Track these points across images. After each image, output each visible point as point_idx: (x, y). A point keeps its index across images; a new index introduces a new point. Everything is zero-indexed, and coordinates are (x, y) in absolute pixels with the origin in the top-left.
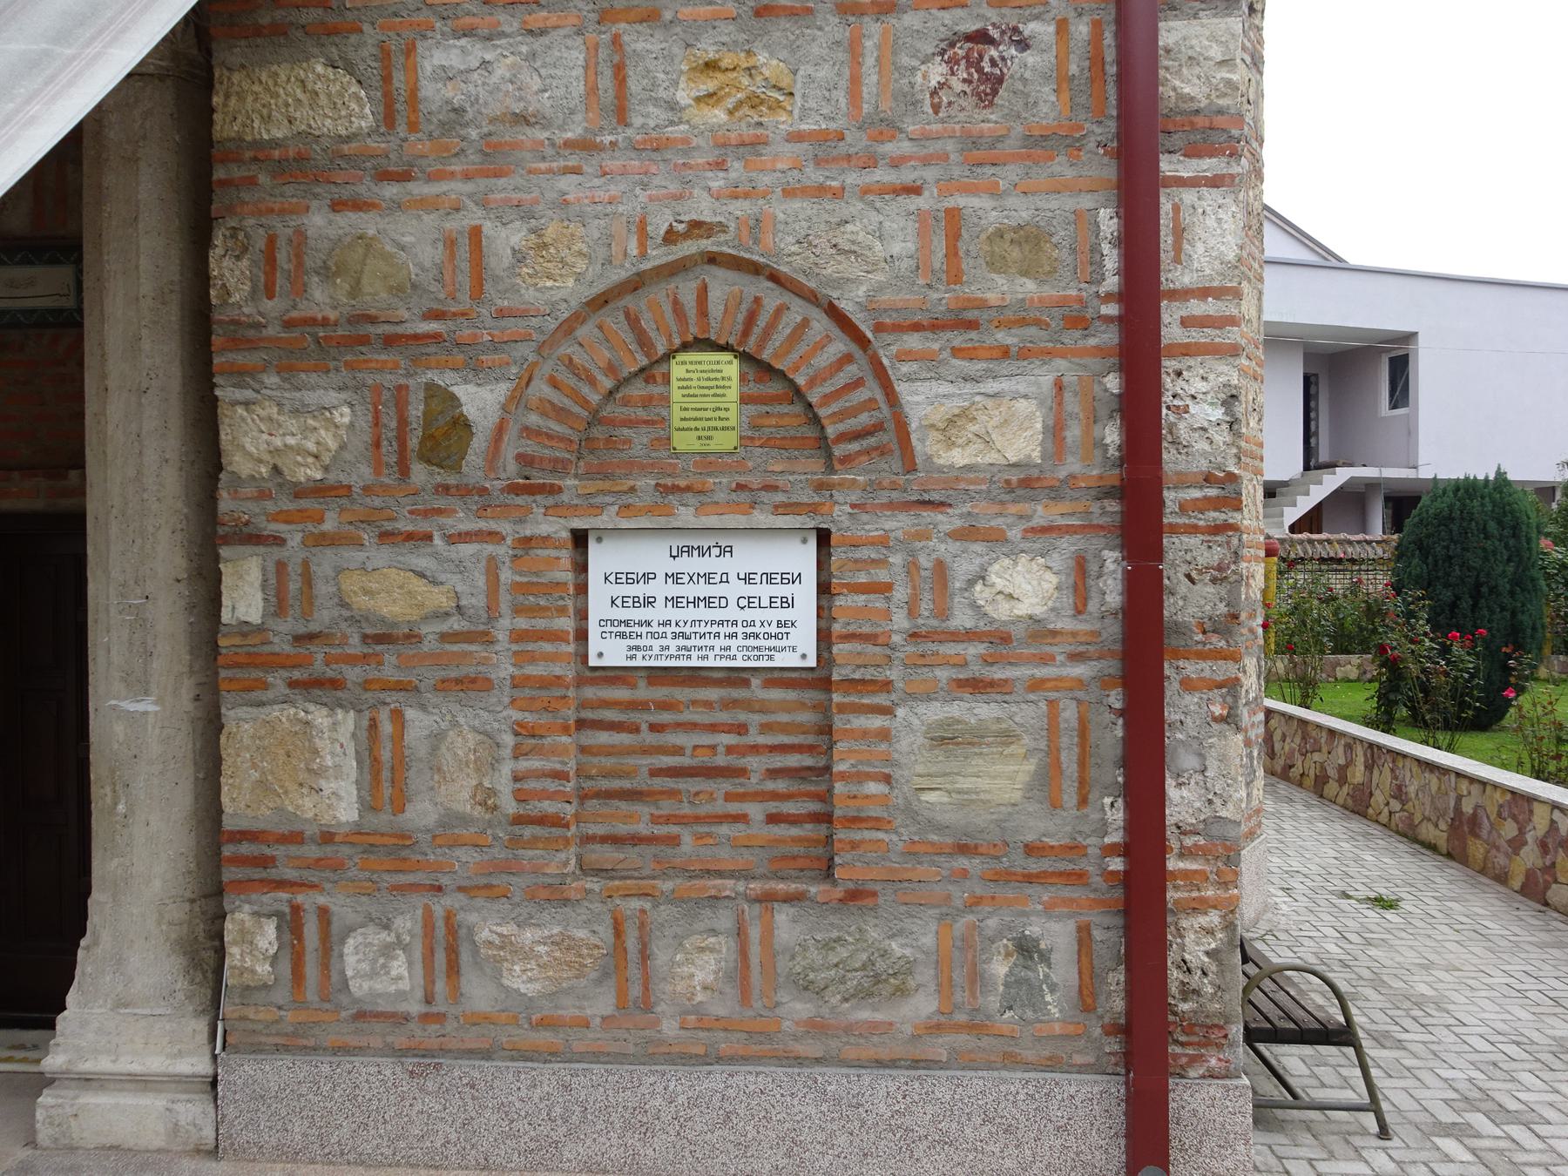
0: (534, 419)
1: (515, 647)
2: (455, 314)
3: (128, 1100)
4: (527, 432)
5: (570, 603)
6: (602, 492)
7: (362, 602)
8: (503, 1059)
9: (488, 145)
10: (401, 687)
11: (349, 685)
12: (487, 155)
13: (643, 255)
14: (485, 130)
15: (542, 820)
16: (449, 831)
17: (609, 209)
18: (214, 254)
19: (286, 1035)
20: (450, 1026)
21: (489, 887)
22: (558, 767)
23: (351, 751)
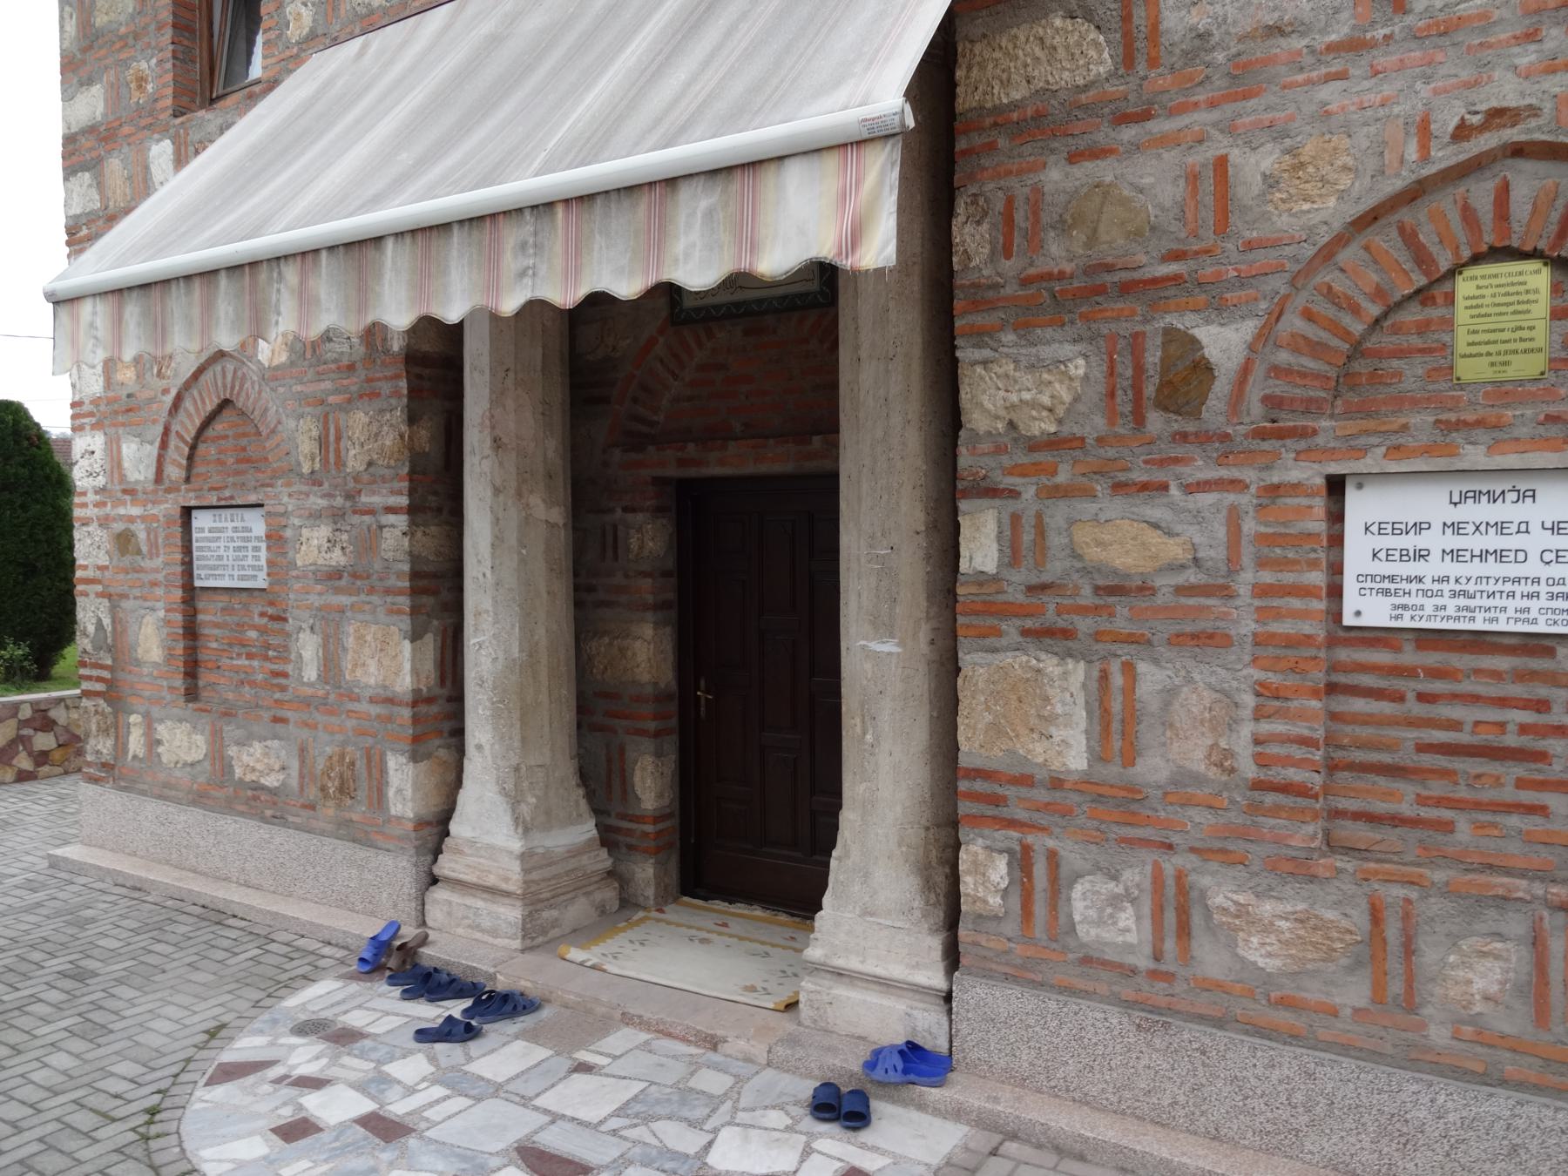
0: (1283, 357)
1: (1257, 603)
2: (1197, 253)
3: (873, 998)
4: (1277, 371)
5: (1322, 555)
6: (1367, 432)
7: (1093, 553)
8: (1238, 1031)
9: (1237, 66)
10: (1131, 639)
11: (1080, 635)
12: (1235, 77)
13: (1425, 157)
14: (1234, 51)
15: (1285, 788)
16: (1181, 790)
17: (1381, 113)
18: (957, 223)
19: (1015, 966)
20: (1180, 987)
21: (1223, 851)
22: (1306, 732)
23: (1081, 700)
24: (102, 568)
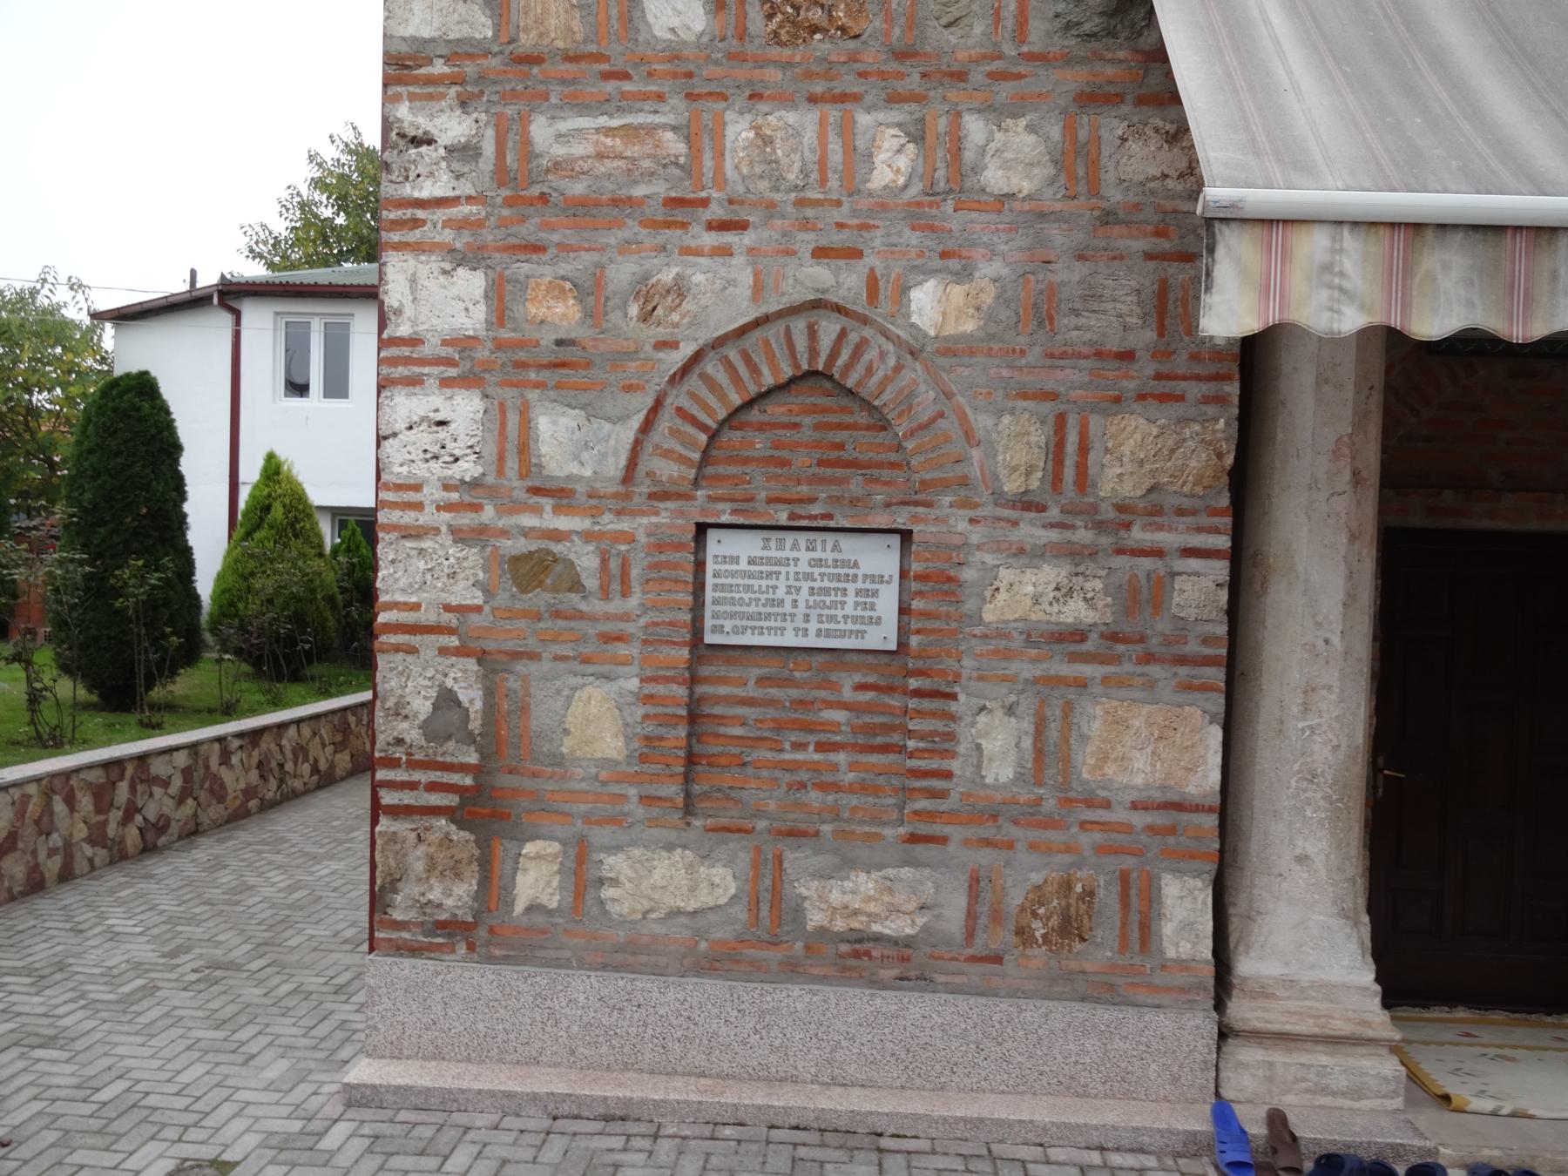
24: (460, 609)
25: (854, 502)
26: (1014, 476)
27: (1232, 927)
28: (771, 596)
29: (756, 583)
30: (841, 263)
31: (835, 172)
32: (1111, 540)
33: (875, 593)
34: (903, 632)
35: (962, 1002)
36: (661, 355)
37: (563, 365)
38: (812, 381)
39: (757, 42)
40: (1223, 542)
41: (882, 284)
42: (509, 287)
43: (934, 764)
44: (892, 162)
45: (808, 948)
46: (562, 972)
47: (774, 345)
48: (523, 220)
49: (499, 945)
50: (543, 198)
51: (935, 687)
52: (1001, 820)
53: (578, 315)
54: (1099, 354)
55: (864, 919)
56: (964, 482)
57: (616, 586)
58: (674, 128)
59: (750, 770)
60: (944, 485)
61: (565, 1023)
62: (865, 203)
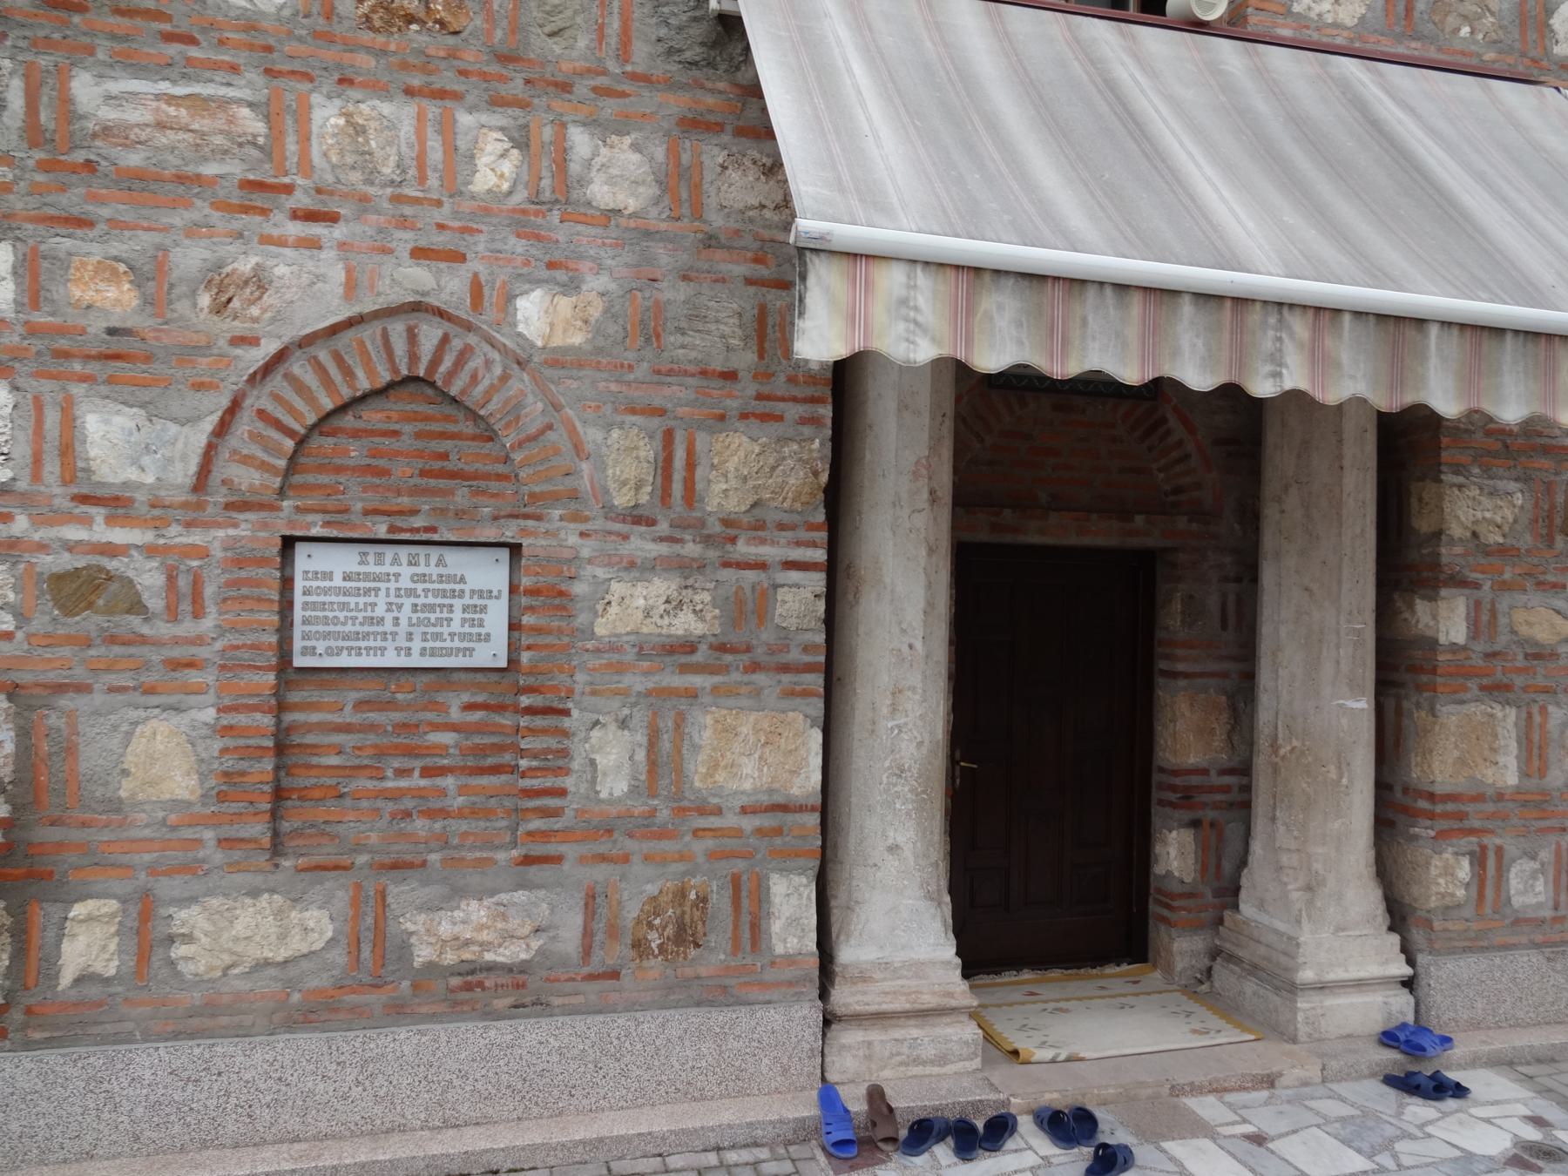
3: (1356, 999)
7: (1524, 630)
10: (1546, 690)
23: (1514, 735)
25: (459, 514)
26: (625, 490)
27: (833, 919)
28: (369, 614)
29: (352, 600)
30: (443, 265)
31: (435, 170)
32: (718, 553)
33: (484, 609)
34: (513, 648)
35: (579, 1023)
36: (238, 351)
37: (116, 357)
38: (412, 388)
39: (346, 23)
40: (820, 555)
41: (486, 291)
42: (45, 264)
43: (548, 782)
44: (495, 167)
45: (415, 986)
46: (123, 1047)
47: (370, 347)
48: (63, 188)
49: (40, 1027)
50: (89, 166)
51: (548, 703)
52: (616, 835)
53: (135, 303)
54: (704, 373)
55: (476, 948)
56: (574, 495)
57: (186, 606)
58: (251, 105)
59: (348, 802)
60: (554, 498)
61: (126, 1106)
62: (467, 206)
